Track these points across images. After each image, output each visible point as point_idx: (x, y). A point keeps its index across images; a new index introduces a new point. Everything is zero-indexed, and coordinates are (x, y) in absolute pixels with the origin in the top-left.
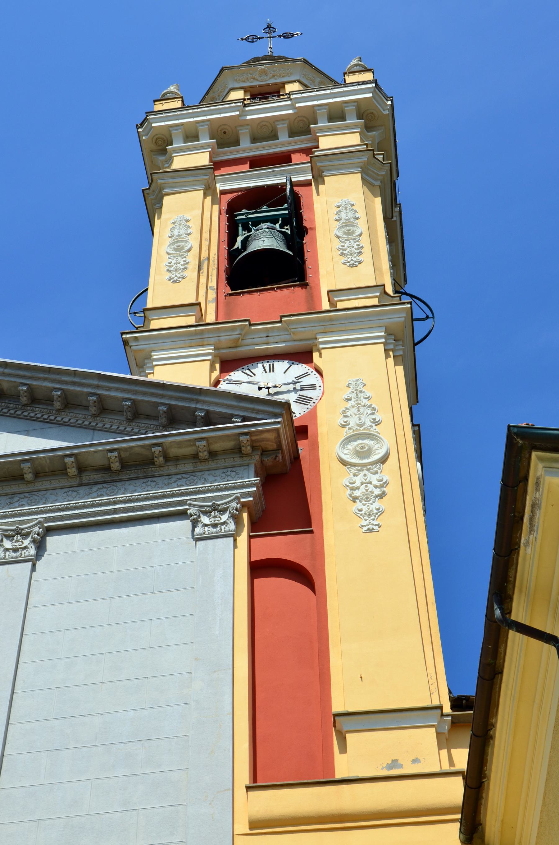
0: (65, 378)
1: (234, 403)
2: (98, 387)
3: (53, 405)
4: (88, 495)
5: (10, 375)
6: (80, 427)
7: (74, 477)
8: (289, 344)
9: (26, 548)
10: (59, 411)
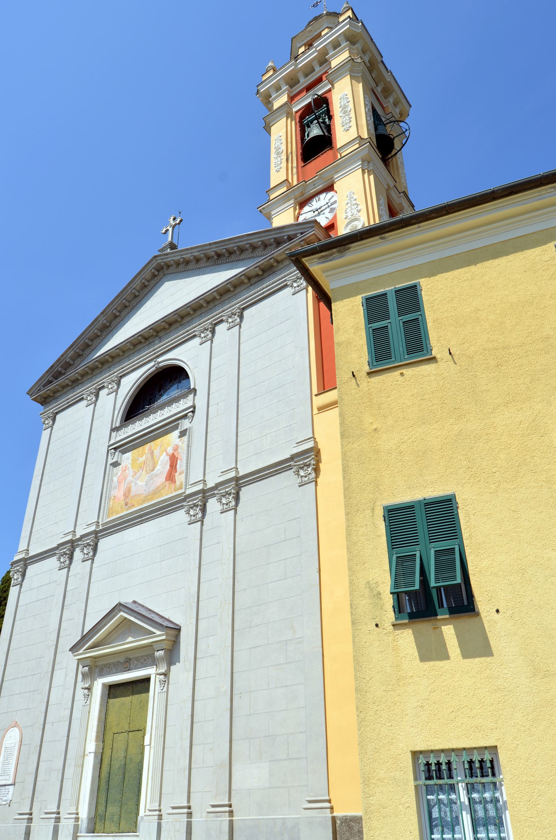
0: (236, 241)
1: (296, 228)
2: (248, 240)
3: (236, 253)
4: (254, 289)
5: (219, 247)
6: (249, 258)
7: (247, 283)
8: (323, 184)
9: (302, 284)
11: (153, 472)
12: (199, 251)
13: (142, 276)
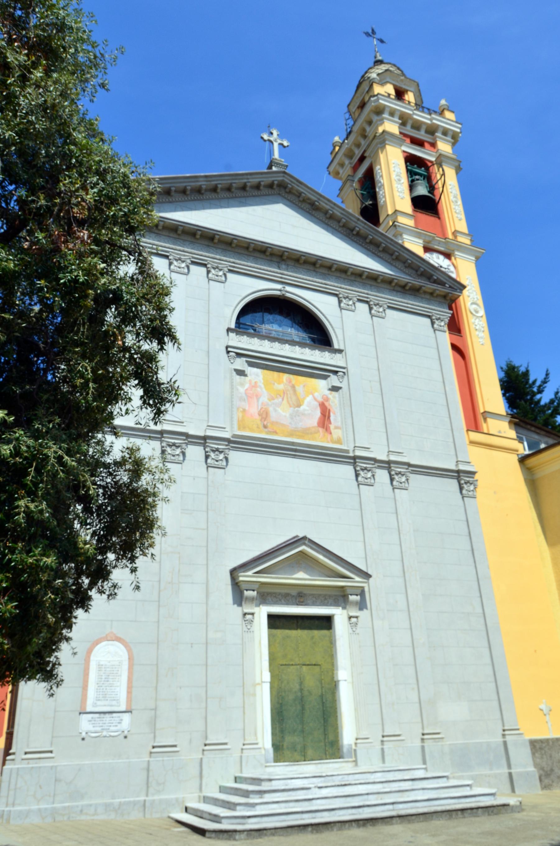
0: (388, 241)
2: (400, 250)
5: (366, 229)
6: (386, 261)
10: (380, 251)
11: (299, 409)
12: (342, 214)
13: (263, 178)
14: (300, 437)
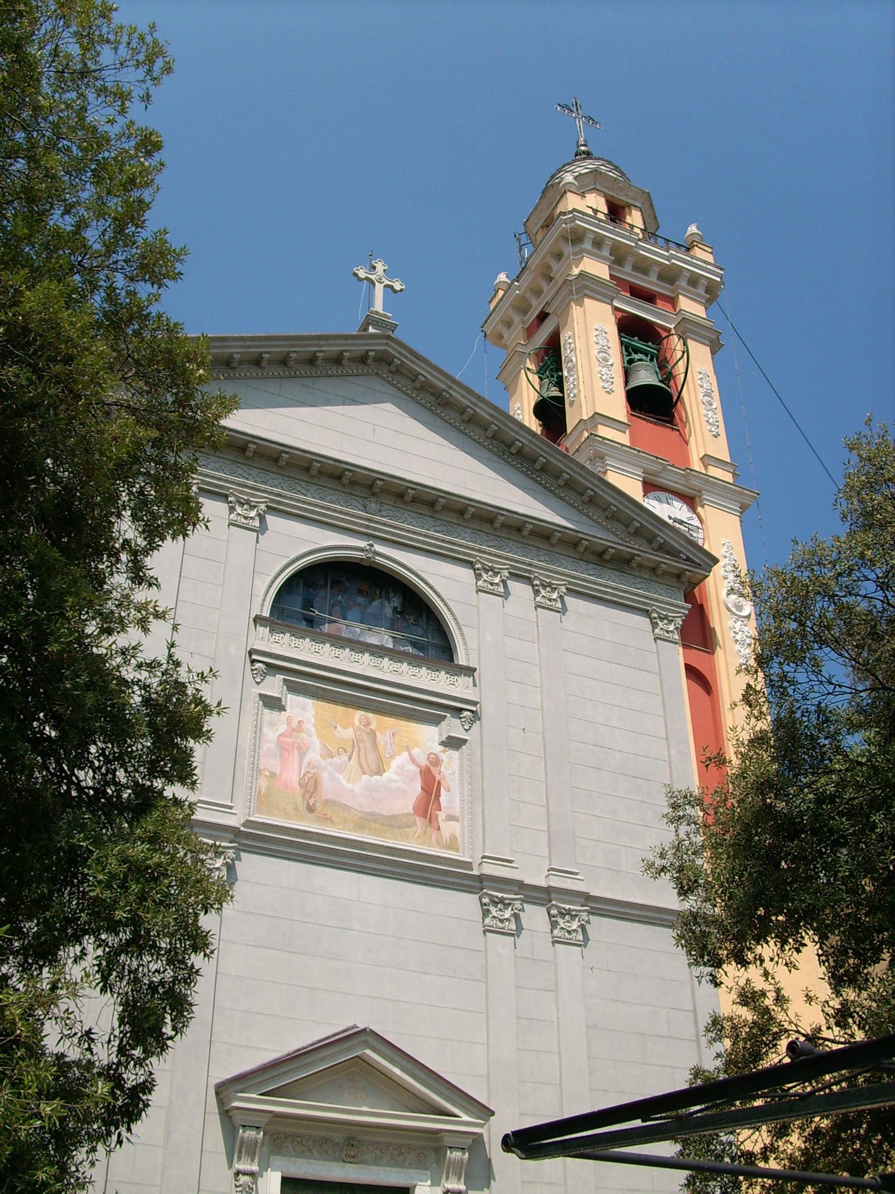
2: (597, 486)
6: (571, 504)
8: (686, 489)
14: (377, 833)
